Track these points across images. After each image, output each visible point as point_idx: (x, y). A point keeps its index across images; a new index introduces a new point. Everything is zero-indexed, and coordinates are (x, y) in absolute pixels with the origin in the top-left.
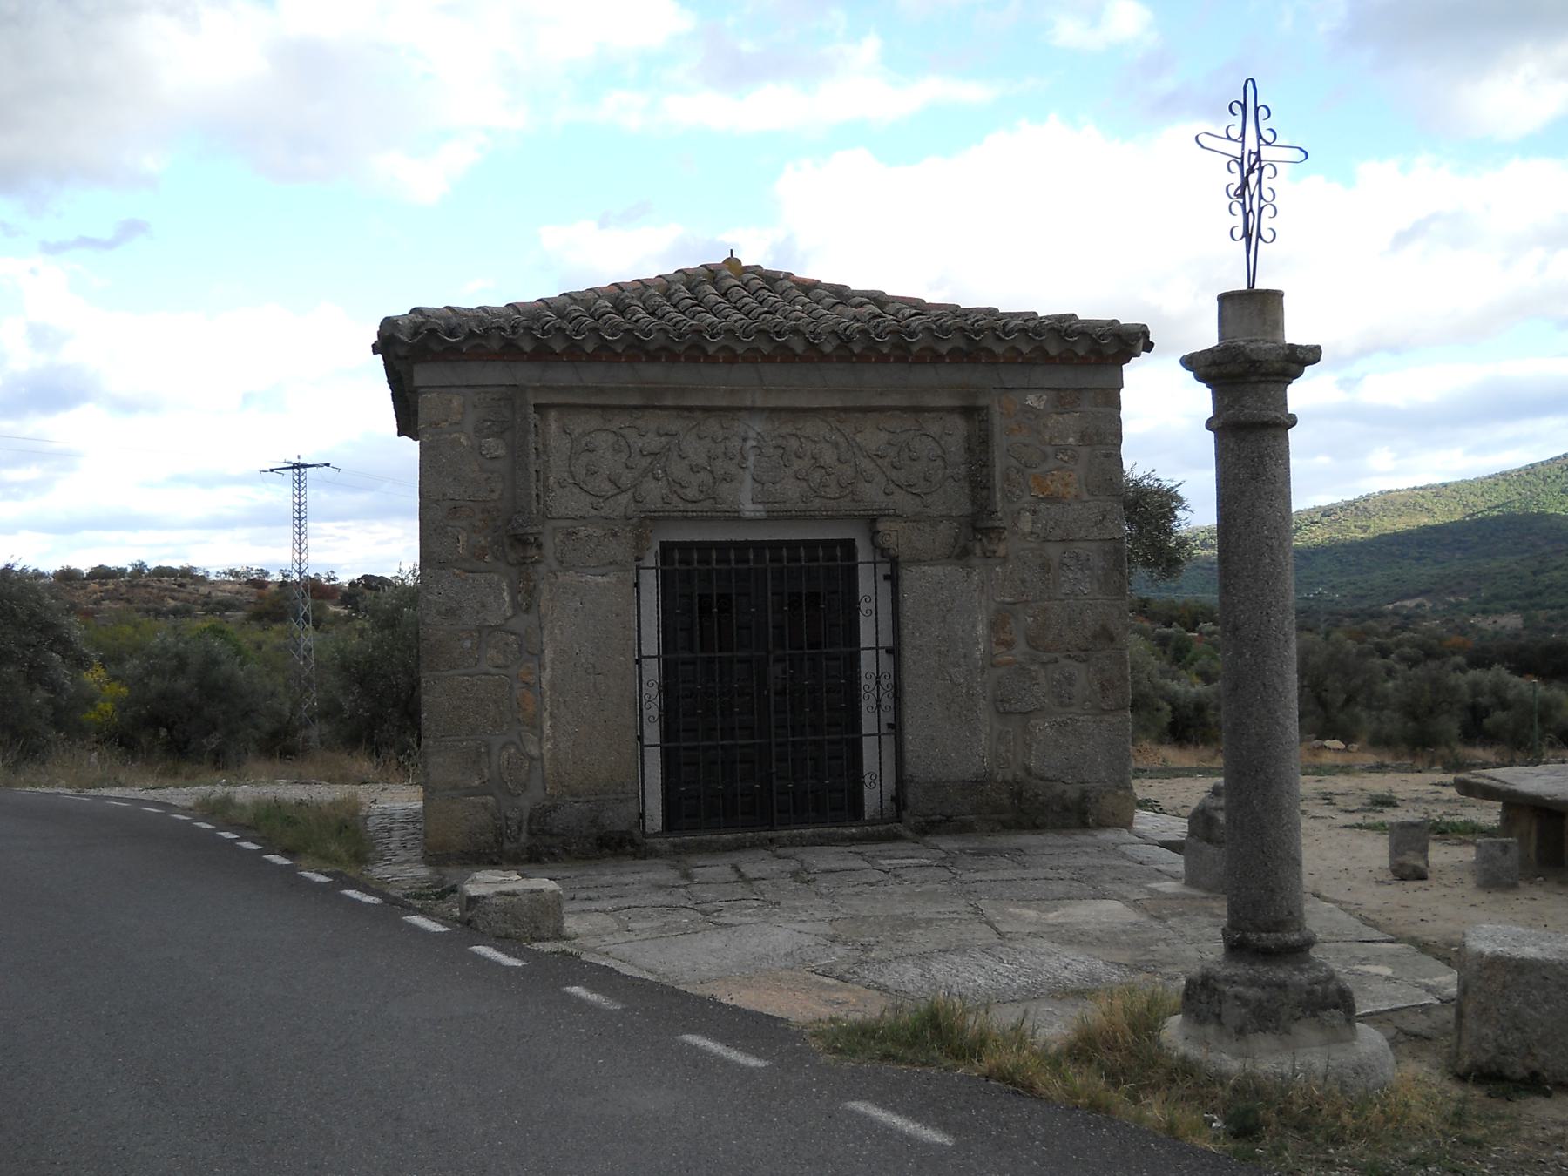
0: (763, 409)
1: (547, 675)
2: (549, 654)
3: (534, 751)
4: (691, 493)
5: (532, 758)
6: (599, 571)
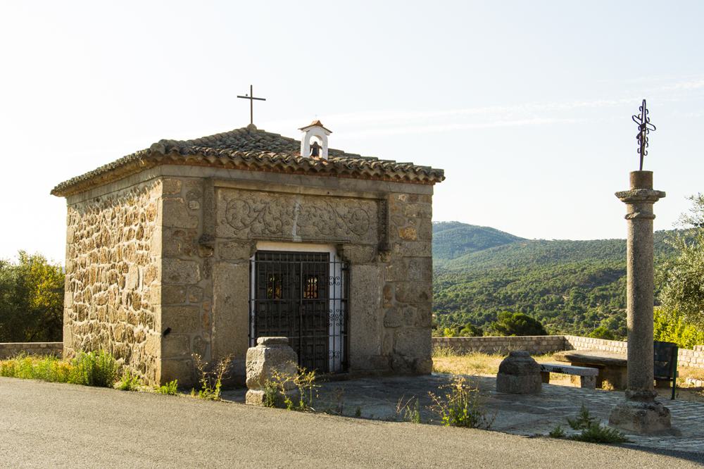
0: (302, 194)
1: (214, 307)
2: (215, 298)
3: (208, 340)
4: (273, 229)
5: (207, 343)
6: (235, 262)
